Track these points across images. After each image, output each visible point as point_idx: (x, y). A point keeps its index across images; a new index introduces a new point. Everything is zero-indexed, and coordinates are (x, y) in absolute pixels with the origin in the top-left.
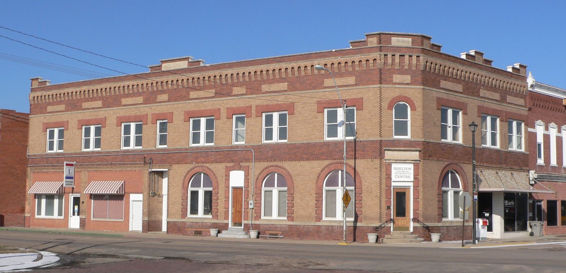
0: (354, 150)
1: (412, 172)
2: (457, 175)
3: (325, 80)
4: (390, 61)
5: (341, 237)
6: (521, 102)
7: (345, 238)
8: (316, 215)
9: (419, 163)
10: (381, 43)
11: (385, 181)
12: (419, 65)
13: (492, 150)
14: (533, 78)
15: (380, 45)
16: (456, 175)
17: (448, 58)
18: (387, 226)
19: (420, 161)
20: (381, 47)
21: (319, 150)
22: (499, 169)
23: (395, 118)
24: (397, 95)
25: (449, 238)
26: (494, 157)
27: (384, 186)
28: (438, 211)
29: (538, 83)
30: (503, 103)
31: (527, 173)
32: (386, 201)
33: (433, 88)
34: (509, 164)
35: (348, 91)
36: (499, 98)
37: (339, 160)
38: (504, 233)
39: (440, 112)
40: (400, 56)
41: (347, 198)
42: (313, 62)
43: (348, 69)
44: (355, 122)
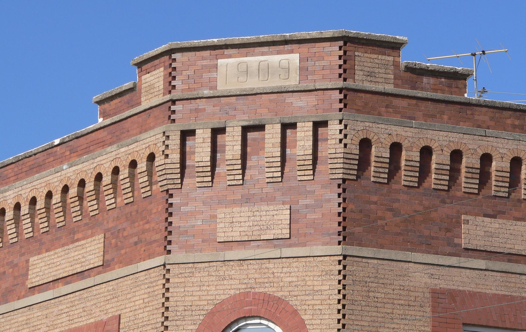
3: (31, 259)
15: (168, 97)
20: (174, 102)
24: (232, 292)
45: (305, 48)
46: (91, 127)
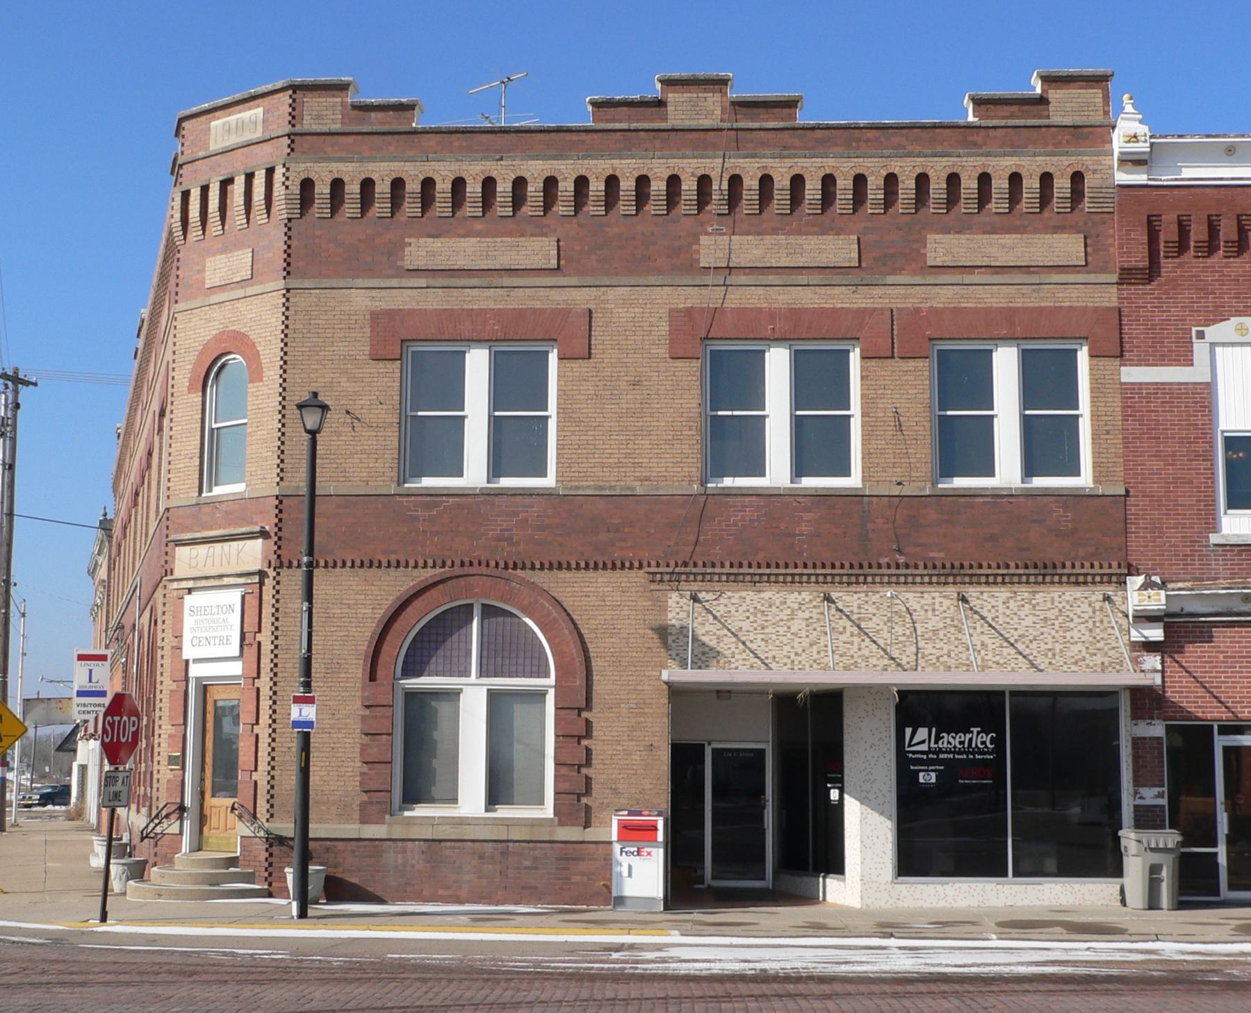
6: (1069, 247)
13: (787, 499)
14: (1141, 122)
24: (214, 332)
25: (441, 892)
29: (1166, 137)
31: (1110, 590)
45: (267, 100)
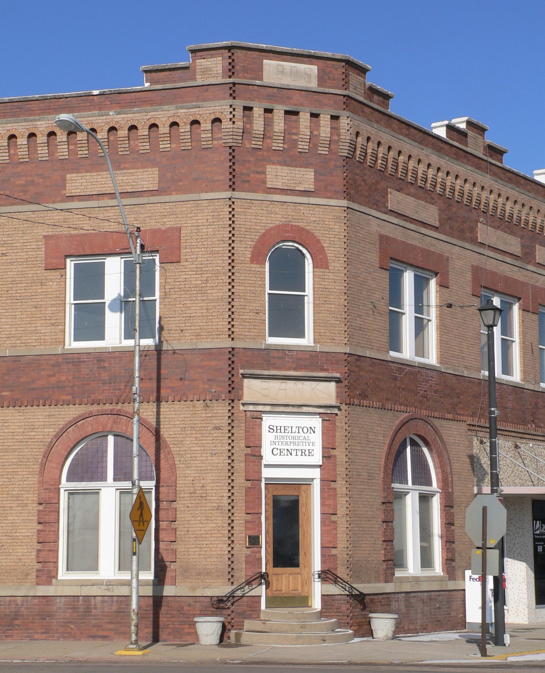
0: (155, 376)
1: (317, 438)
2: (425, 450)
3: (68, 176)
4: (258, 125)
5: (113, 630)
7: (137, 635)
8: (39, 566)
9: (337, 414)
10: (233, 73)
11: (243, 465)
12: (338, 141)
13: (505, 387)
15: (231, 80)
16: (422, 450)
17: (407, 132)
18: (252, 593)
19: (340, 409)
20: (234, 84)
21: (49, 376)
22: (520, 435)
23: (270, 289)
24: (278, 223)
25: (411, 627)
26: (510, 405)
27: (240, 479)
28: (385, 549)
30: (528, 264)
32: (247, 522)
33: (370, 208)
34: (541, 425)
35: (137, 209)
36: (520, 250)
37: (107, 405)
38: (536, 608)
39: (386, 275)
40: (287, 112)
41: (141, 514)
42: (35, 123)
43: (137, 145)
44: (157, 296)
45: (321, 62)
46: (139, 88)
